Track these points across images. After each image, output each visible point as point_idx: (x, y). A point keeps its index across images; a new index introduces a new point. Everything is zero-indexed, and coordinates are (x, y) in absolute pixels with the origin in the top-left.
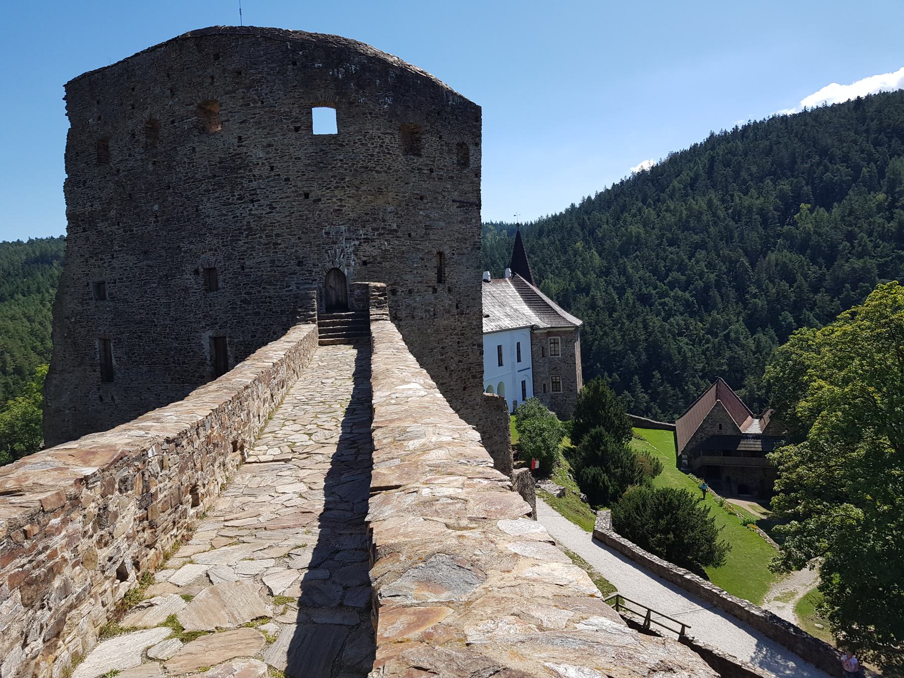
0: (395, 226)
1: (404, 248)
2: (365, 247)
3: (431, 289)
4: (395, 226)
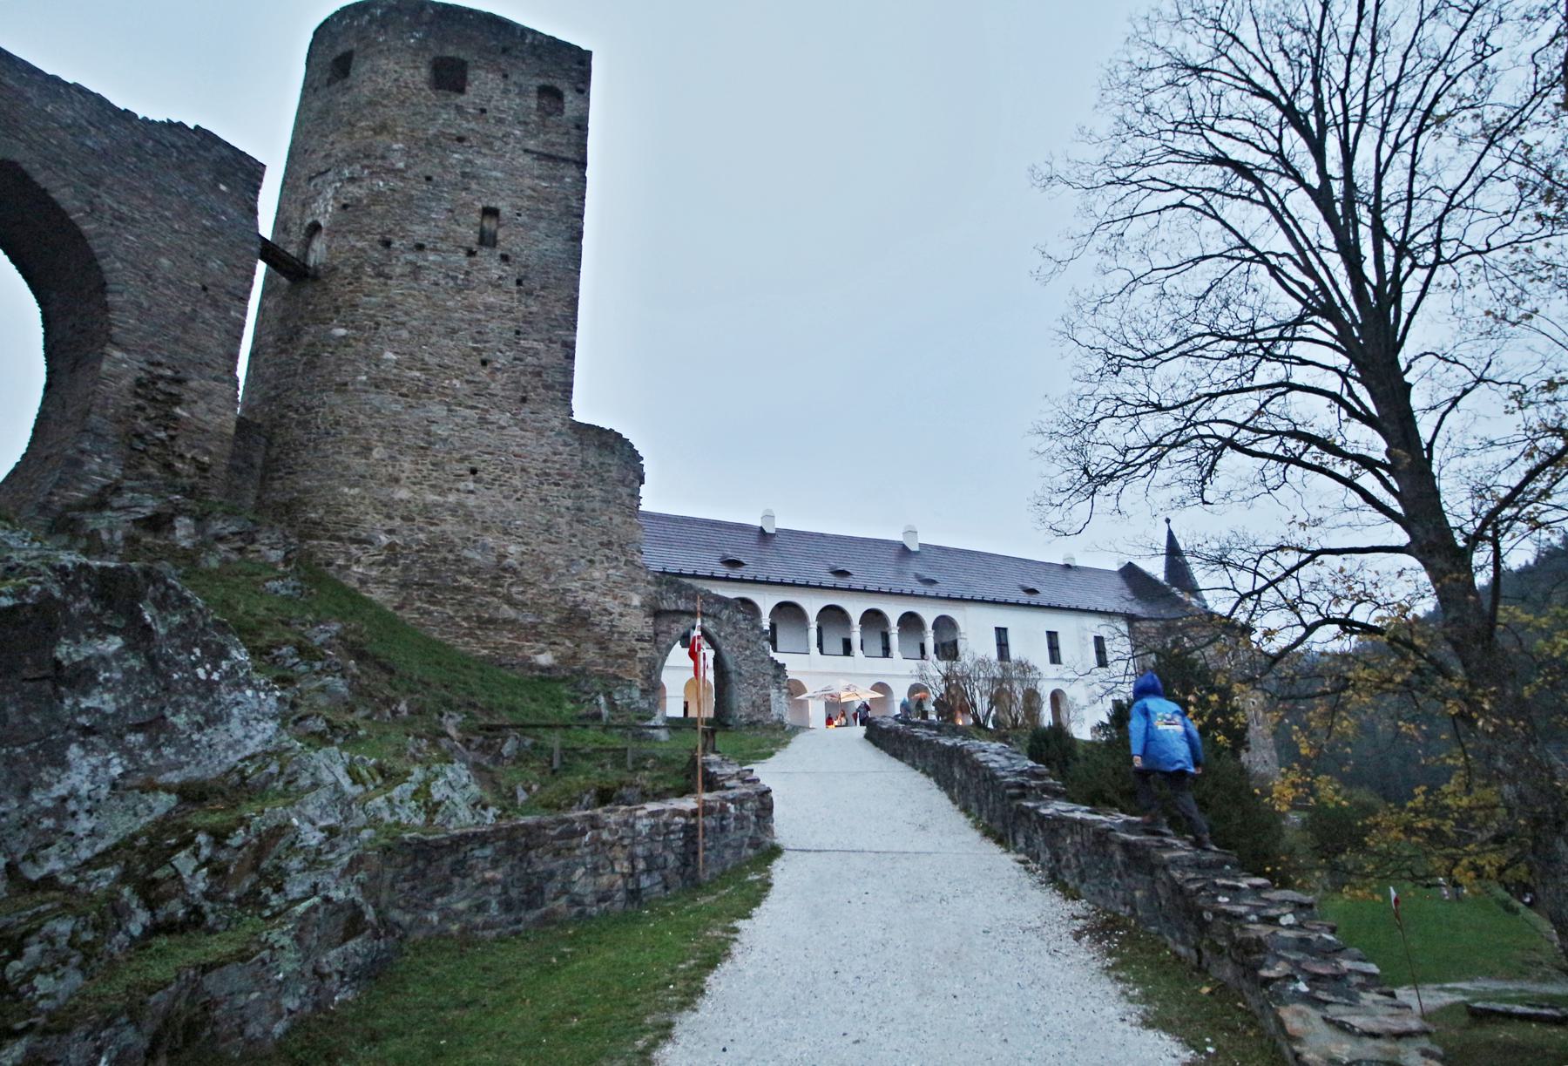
0: (401, 165)
2: (353, 189)
3: (462, 254)
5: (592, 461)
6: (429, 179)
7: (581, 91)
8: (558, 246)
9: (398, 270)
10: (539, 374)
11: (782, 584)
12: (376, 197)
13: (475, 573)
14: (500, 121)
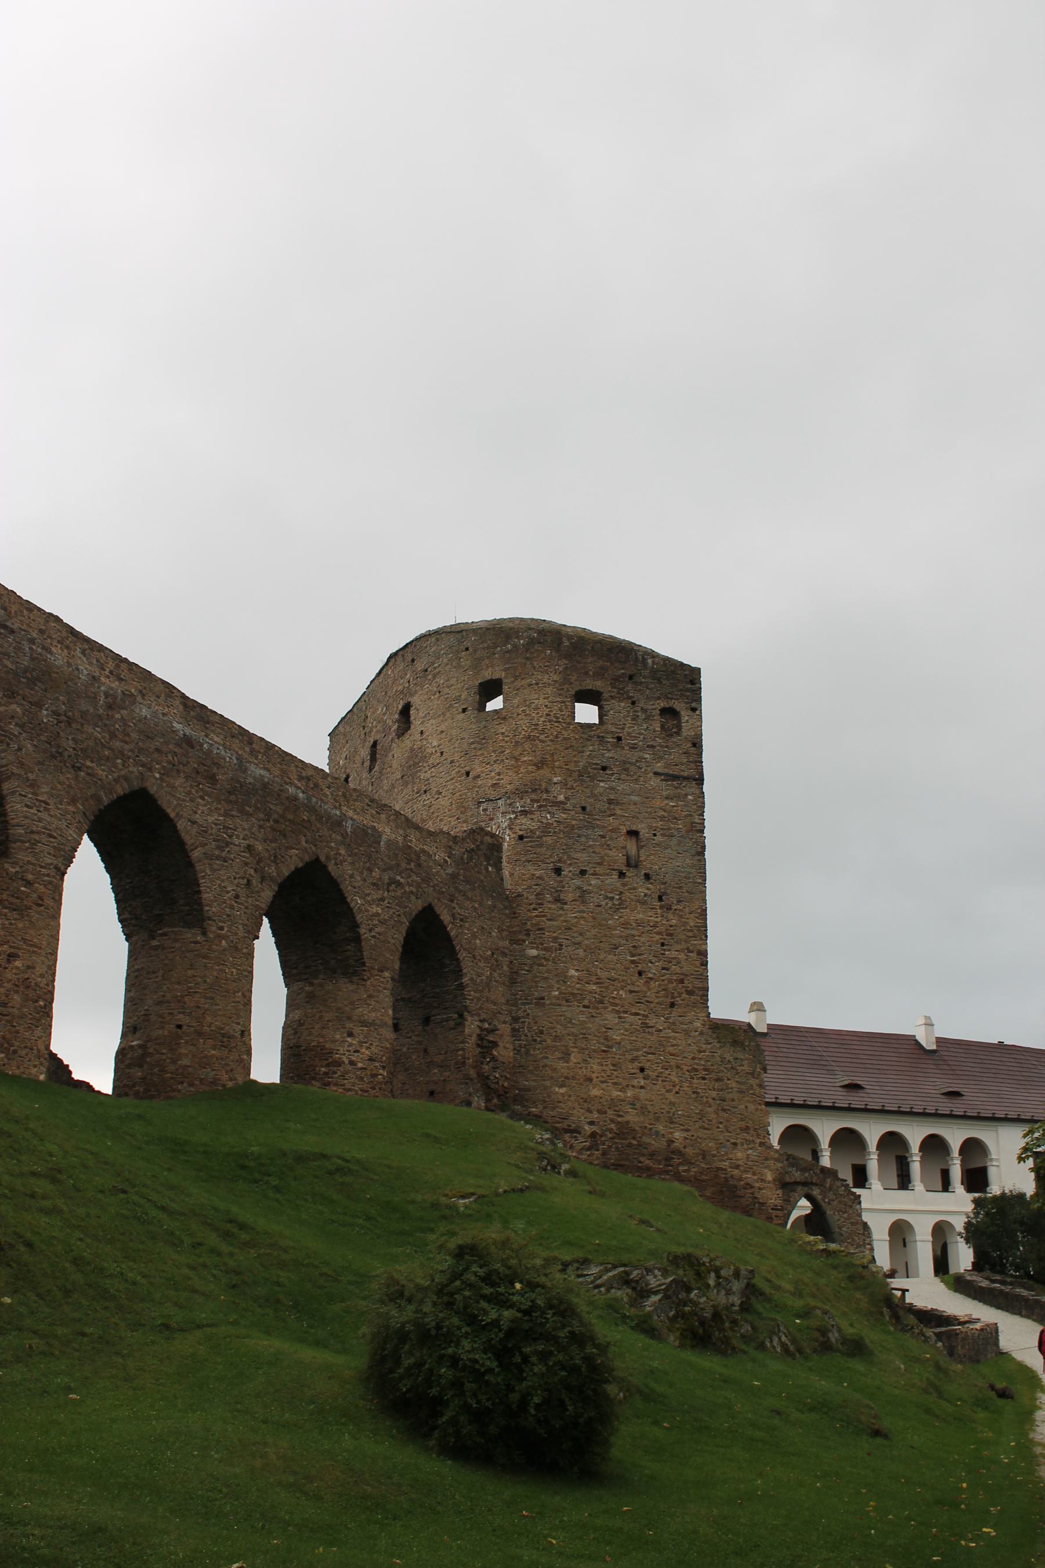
0: (561, 798)
1: (574, 822)
2: (523, 820)
5: (728, 1057)
6: (584, 808)
7: (694, 710)
8: (688, 861)
9: (570, 897)
10: (682, 981)
11: (792, 1105)
12: (546, 829)
13: (652, 1155)
14: (633, 747)
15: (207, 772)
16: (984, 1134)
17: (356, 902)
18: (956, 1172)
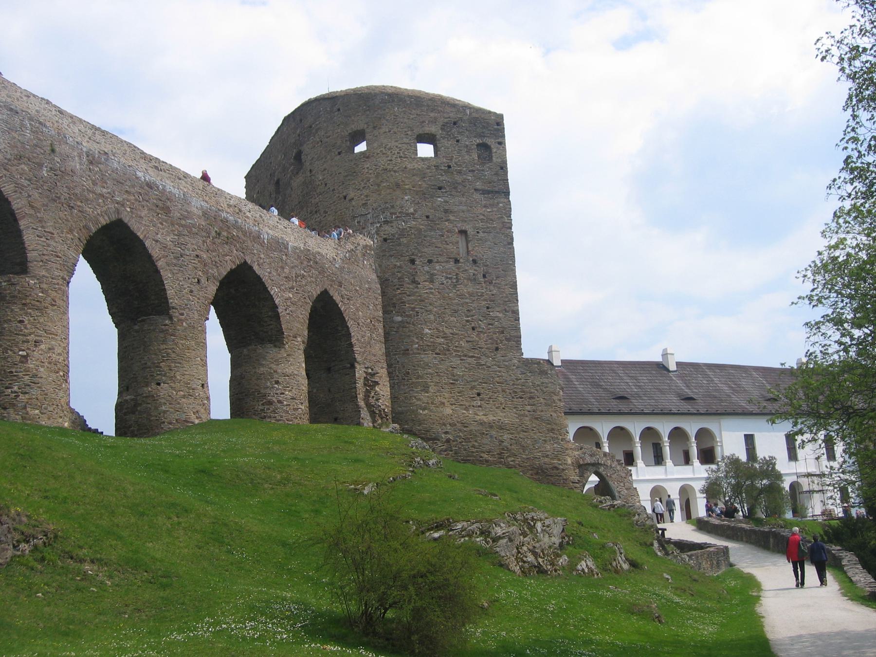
0: (412, 210)
4: (412, 210)
6: (428, 217)
12: (403, 233)
14: (460, 172)
15: (163, 205)
16: (710, 424)
17: (274, 291)
18: (694, 451)
